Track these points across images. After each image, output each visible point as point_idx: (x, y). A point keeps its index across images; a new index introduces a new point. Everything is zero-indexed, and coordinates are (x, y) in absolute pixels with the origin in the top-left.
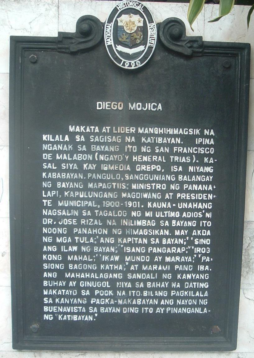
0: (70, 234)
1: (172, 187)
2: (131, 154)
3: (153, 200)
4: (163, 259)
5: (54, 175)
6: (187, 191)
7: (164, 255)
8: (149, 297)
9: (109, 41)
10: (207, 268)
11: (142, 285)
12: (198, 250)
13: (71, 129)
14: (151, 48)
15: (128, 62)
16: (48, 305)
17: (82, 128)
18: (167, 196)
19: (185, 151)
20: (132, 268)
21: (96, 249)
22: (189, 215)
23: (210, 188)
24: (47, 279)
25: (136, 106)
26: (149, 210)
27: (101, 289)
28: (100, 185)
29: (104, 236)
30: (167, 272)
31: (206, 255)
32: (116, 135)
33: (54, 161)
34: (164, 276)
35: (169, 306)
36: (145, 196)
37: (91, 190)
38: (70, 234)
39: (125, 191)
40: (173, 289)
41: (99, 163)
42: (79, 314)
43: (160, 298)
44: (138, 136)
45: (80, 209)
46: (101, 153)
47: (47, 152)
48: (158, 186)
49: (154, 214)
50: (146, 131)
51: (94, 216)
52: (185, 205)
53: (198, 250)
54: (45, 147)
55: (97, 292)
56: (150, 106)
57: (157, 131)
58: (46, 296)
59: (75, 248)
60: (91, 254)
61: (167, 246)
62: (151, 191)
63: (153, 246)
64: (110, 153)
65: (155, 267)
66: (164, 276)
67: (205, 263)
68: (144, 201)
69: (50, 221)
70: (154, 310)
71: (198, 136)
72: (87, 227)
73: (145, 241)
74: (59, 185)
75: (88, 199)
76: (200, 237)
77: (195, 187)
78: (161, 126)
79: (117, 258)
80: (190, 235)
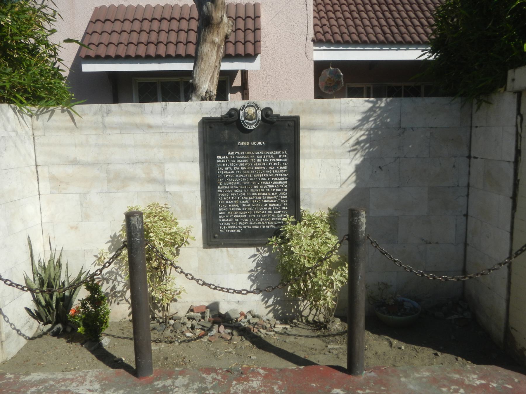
0: (230, 196)
1: (270, 175)
2: (253, 162)
3: (262, 181)
4: (268, 205)
5: (222, 172)
6: (277, 177)
7: (268, 203)
8: (263, 221)
9: (242, 118)
10: (286, 208)
11: (260, 216)
12: (282, 201)
13: (229, 153)
14: (259, 120)
15: (250, 126)
16: (222, 226)
17: (233, 153)
18: (268, 179)
19: (275, 160)
20: (255, 209)
21: (240, 202)
22: (278, 186)
23: (286, 175)
24: (221, 215)
25: (255, 143)
26: (261, 185)
27: (243, 218)
28: (241, 175)
29: (243, 196)
30: (270, 210)
31: (285, 203)
32: (247, 155)
33: (222, 167)
34: (269, 212)
35: (271, 225)
36: (259, 179)
37: (237, 178)
38: (230, 196)
39: (251, 177)
40: (273, 217)
41: (240, 167)
42: (234, 229)
43: (268, 221)
44: (255, 155)
45: (233, 185)
46: (241, 163)
47: (219, 163)
48: (265, 175)
49: (263, 187)
50: (259, 153)
51: (239, 188)
52: (276, 183)
53: (282, 201)
54: (218, 161)
55: (241, 220)
56: (260, 143)
57: (263, 153)
58: (220, 222)
59: (232, 202)
60: (238, 204)
61: (269, 199)
62: (262, 177)
63: (264, 200)
64: (244, 163)
65: (265, 208)
66: (269, 212)
67: (285, 206)
68: (259, 181)
69: (221, 191)
70: (266, 227)
71: (280, 154)
72: (237, 193)
73: (260, 198)
74: (224, 176)
75: (237, 182)
76: (283, 195)
77: (280, 175)
78: (264, 151)
79: (249, 205)
80: (278, 194)
